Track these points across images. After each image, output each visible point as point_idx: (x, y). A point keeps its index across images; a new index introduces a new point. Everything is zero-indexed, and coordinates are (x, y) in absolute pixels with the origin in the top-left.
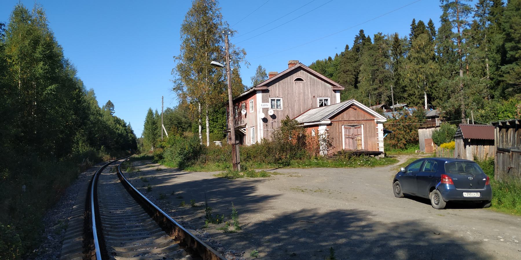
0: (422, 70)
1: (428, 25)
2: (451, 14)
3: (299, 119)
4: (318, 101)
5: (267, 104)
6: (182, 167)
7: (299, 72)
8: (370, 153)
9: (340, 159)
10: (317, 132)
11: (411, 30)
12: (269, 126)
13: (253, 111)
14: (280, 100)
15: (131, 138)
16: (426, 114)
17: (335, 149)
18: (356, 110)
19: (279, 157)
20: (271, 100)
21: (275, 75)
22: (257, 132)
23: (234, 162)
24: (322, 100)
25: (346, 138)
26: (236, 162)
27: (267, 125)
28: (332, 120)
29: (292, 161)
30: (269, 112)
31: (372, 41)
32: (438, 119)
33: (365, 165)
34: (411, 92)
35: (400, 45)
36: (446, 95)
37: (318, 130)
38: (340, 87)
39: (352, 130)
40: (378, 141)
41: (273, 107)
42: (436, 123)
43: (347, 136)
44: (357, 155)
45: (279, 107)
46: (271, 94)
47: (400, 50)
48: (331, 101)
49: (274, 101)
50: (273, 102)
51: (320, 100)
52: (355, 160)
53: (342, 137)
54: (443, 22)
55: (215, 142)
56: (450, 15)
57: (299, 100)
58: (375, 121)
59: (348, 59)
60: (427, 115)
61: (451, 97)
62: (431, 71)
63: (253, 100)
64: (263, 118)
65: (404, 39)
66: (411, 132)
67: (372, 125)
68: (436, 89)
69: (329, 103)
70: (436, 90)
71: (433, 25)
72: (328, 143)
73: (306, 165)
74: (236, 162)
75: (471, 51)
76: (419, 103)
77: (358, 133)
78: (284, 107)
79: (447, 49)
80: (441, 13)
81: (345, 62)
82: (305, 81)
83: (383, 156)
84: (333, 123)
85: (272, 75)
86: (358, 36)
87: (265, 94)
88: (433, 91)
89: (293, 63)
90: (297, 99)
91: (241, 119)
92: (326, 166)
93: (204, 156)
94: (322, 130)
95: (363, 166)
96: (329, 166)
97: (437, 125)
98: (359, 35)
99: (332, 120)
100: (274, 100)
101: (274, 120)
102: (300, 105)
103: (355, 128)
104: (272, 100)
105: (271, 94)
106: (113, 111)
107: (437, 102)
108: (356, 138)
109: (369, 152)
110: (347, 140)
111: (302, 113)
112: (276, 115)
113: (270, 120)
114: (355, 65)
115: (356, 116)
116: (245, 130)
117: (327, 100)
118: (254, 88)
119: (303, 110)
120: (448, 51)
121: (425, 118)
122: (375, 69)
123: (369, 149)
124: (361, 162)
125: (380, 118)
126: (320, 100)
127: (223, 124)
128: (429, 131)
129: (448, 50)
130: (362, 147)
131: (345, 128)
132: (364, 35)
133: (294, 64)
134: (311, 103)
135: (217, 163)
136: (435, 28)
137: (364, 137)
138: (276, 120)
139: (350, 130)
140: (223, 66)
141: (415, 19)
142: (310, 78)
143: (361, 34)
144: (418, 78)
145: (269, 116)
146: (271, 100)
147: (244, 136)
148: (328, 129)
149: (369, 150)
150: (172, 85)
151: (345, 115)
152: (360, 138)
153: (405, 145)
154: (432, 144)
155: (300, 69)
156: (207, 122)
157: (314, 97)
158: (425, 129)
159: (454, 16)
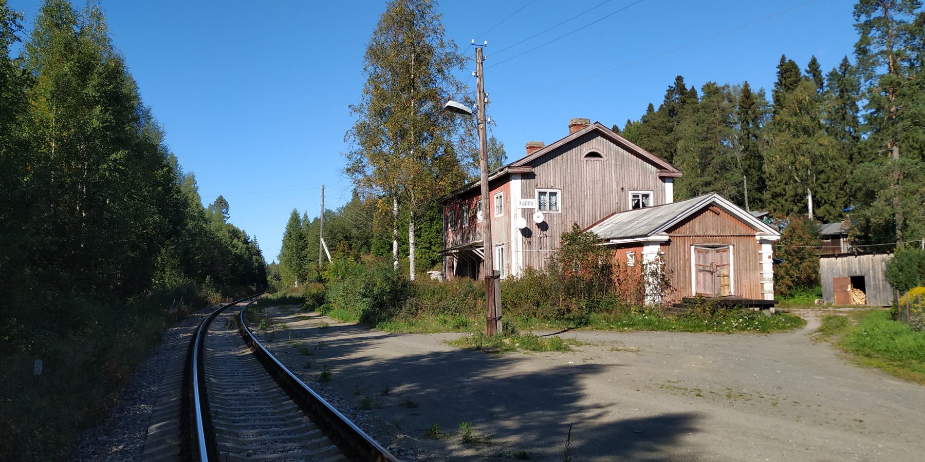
0: (804, 147)
1: (809, 67)
2: (877, 40)
3: (600, 231)
4: (630, 197)
6: (368, 321)
7: (594, 140)
8: (754, 303)
9: (693, 314)
10: (639, 260)
11: (778, 76)
12: (534, 244)
13: (502, 215)
14: (556, 193)
15: (257, 264)
16: (821, 231)
17: (676, 293)
18: (718, 214)
19: (565, 306)
20: (540, 193)
21: (541, 148)
22: (509, 256)
23: (489, 316)
24: (638, 196)
25: (698, 271)
26: (494, 317)
27: (530, 243)
28: (671, 235)
29: (593, 316)
30: (535, 216)
31: (700, 94)
32: (845, 239)
33: (749, 329)
34: (778, 190)
35: (753, 103)
36: (842, 196)
37: (643, 253)
38: (674, 172)
39: (712, 256)
40: (762, 279)
41: (542, 207)
42: (840, 248)
43: (701, 268)
44: (727, 306)
45: (554, 208)
46: (539, 182)
47: (754, 112)
48: (656, 199)
49: (545, 195)
50: (542, 197)
52: (724, 316)
53: (690, 270)
54: (859, 54)
55: (430, 274)
56: (875, 40)
57: (594, 194)
58: (758, 238)
59: (655, 128)
60: (823, 233)
61: (876, 198)
62: (822, 151)
63: (502, 194)
64: (523, 227)
65: (759, 94)
66: (801, 263)
67: (751, 245)
68: (823, 185)
69: (651, 202)
70: (822, 188)
71: (818, 68)
72: (662, 280)
73: (625, 325)
74: (494, 317)
75: (918, 109)
76: (792, 211)
77: (721, 262)
78: (564, 209)
79: (844, 112)
80: (856, 37)
81: (648, 134)
82: (605, 158)
83: (772, 310)
84: (672, 240)
85: (534, 147)
86: (672, 87)
87: (527, 181)
88: (817, 189)
89: (579, 123)
90: (588, 192)
91: (475, 231)
92: (669, 329)
93: (413, 300)
94: (650, 253)
95: (743, 329)
96: (675, 329)
97: (843, 252)
98: (674, 86)
99: (671, 235)
100: (545, 193)
101: (545, 232)
102: (594, 205)
103: (717, 252)
104: (541, 194)
105: (539, 182)
106: (227, 215)
107: (825, 209)
108: (718, 272)
109: (751, 301)
110: (701, 275)
111: (599, 220)
112: (547, 223)
113: (536, 232)
114: (667, 139)
115: (719, 226)
116: (482, 251)
117: (647, 196)
118: (507, 169)
119: (600, 215)
120: (846, 116)
121: (818, 237)
122: (708, 146)
123: (744, 295)
124: (741, 320)
125: (768, 232)
126: (634, 196)
127: (432, 240)
128: (842, 263)
129: (845, 113)
130: (731, 291)
131: (698, 251)
132: (684, 86)
133: (581, 125)
134: (617, 201)
135: (441, 317)
136: (822, 74)
137: (734, 270)
138: (548, 233)
139: (707, 255)
140: (470, 111)
141: (786, 56)
142: (616, 152)
143: (678, 83)
144: (797, 163)
145: (534, 224)
146: (540, 193)
147: (481, 264)
148: (662, 253)
149: (744, 297)
150: (345, 163)
151: (697, 224)
152: (726, 273)
153: (790, 288)
154: (847, 288)
155: (595, 133)
156: (411, 234)
157: (623, 189)
158: (833, 259)
159: (883, 44)
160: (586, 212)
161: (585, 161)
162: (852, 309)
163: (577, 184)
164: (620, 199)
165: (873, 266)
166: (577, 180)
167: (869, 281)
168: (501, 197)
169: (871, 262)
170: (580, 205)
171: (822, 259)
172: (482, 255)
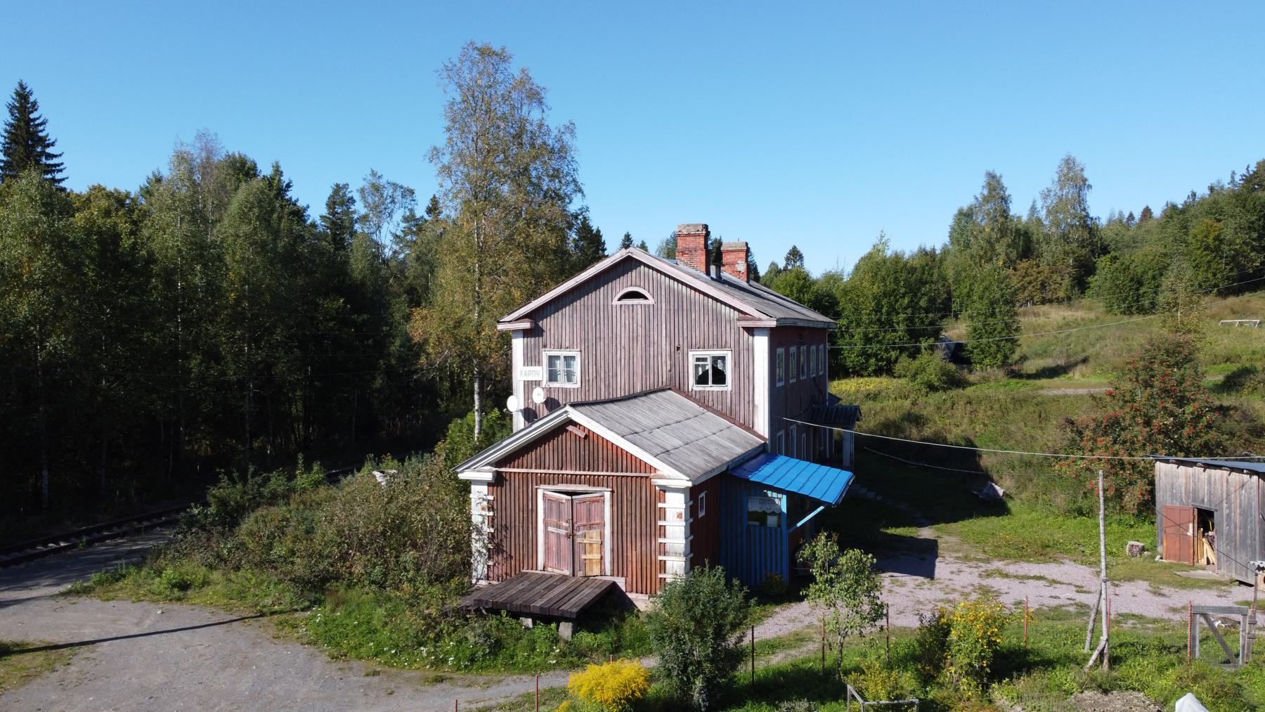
4: (692, 362)
24: (704, 360)
38: (760, 320)
51: (698, 360)
82: (651, 301)
89: (685, 232)
102: (632, 375)
104: (552, 359)
160: (619, 386)
161: (618, 308)
162: (1178, 573)
163: (606, 342)
164: (673, 366)
165: (1228, 495)
166: (606, 336)
167: (1222, 522)
169: (1225, 484)
170: (611, 374)
171: (1158, 462)
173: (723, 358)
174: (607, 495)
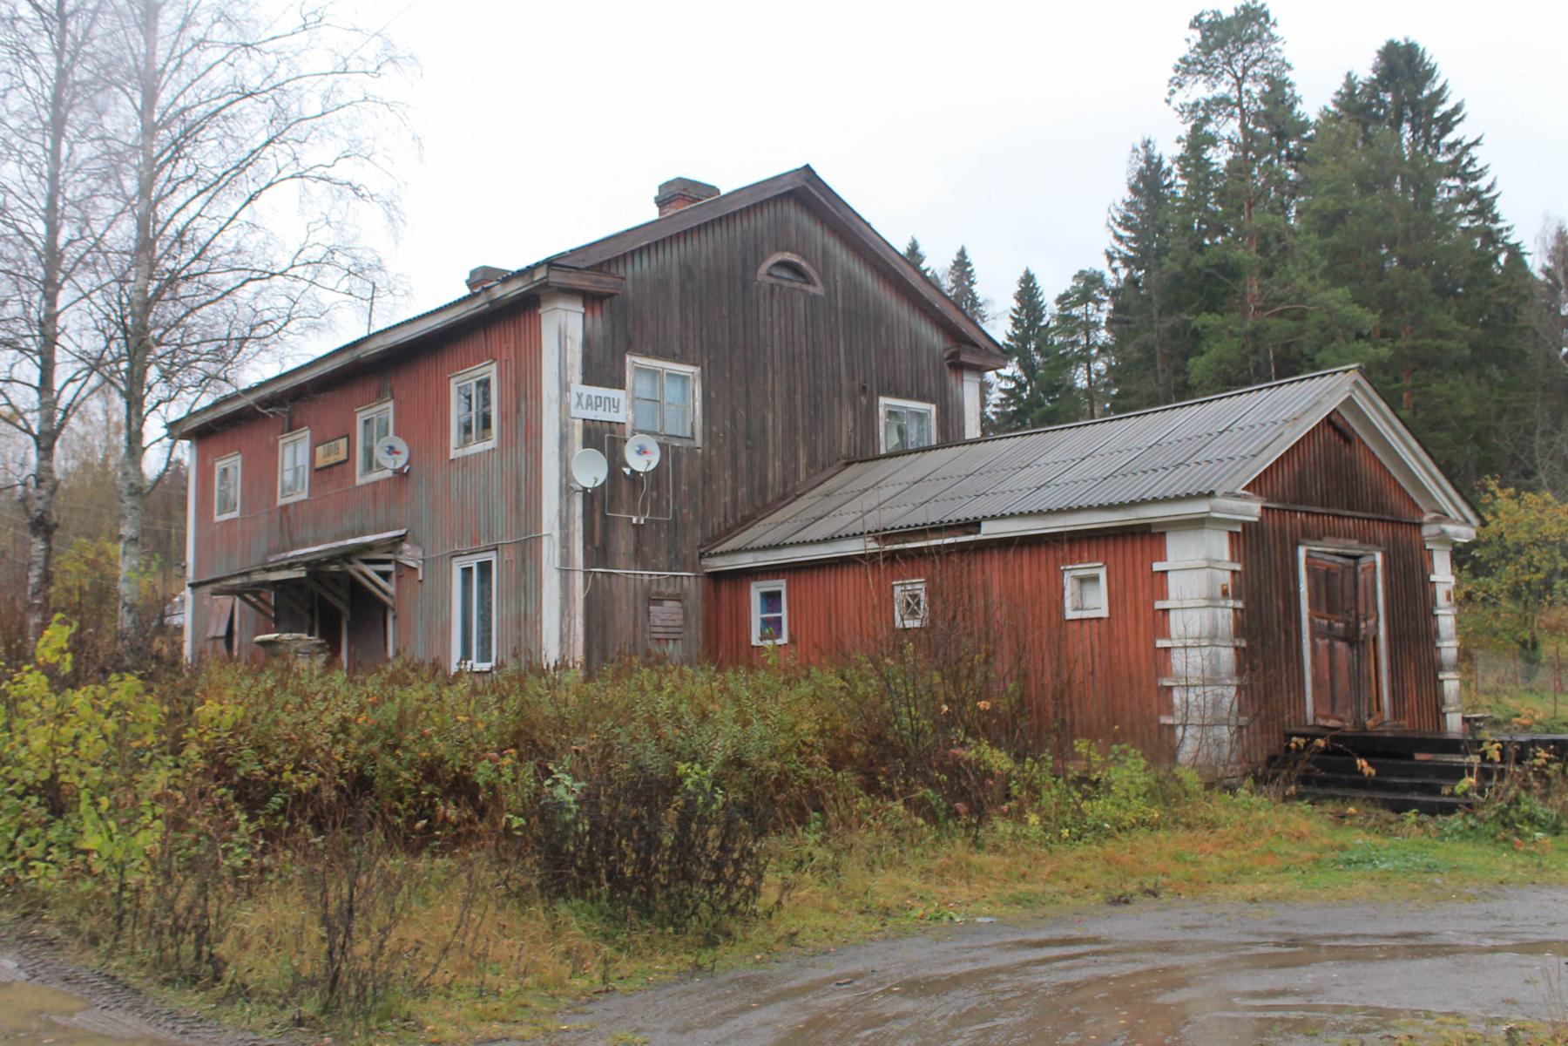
5: (615, 393)
13: (489, 445)
51: (892, 414)
63: (491, 371)
116: (385, 576)
125: (1453, 513)
168: (485, 384)
172: (386, 593)
173: (920, 416)
174: (1379, 557)
